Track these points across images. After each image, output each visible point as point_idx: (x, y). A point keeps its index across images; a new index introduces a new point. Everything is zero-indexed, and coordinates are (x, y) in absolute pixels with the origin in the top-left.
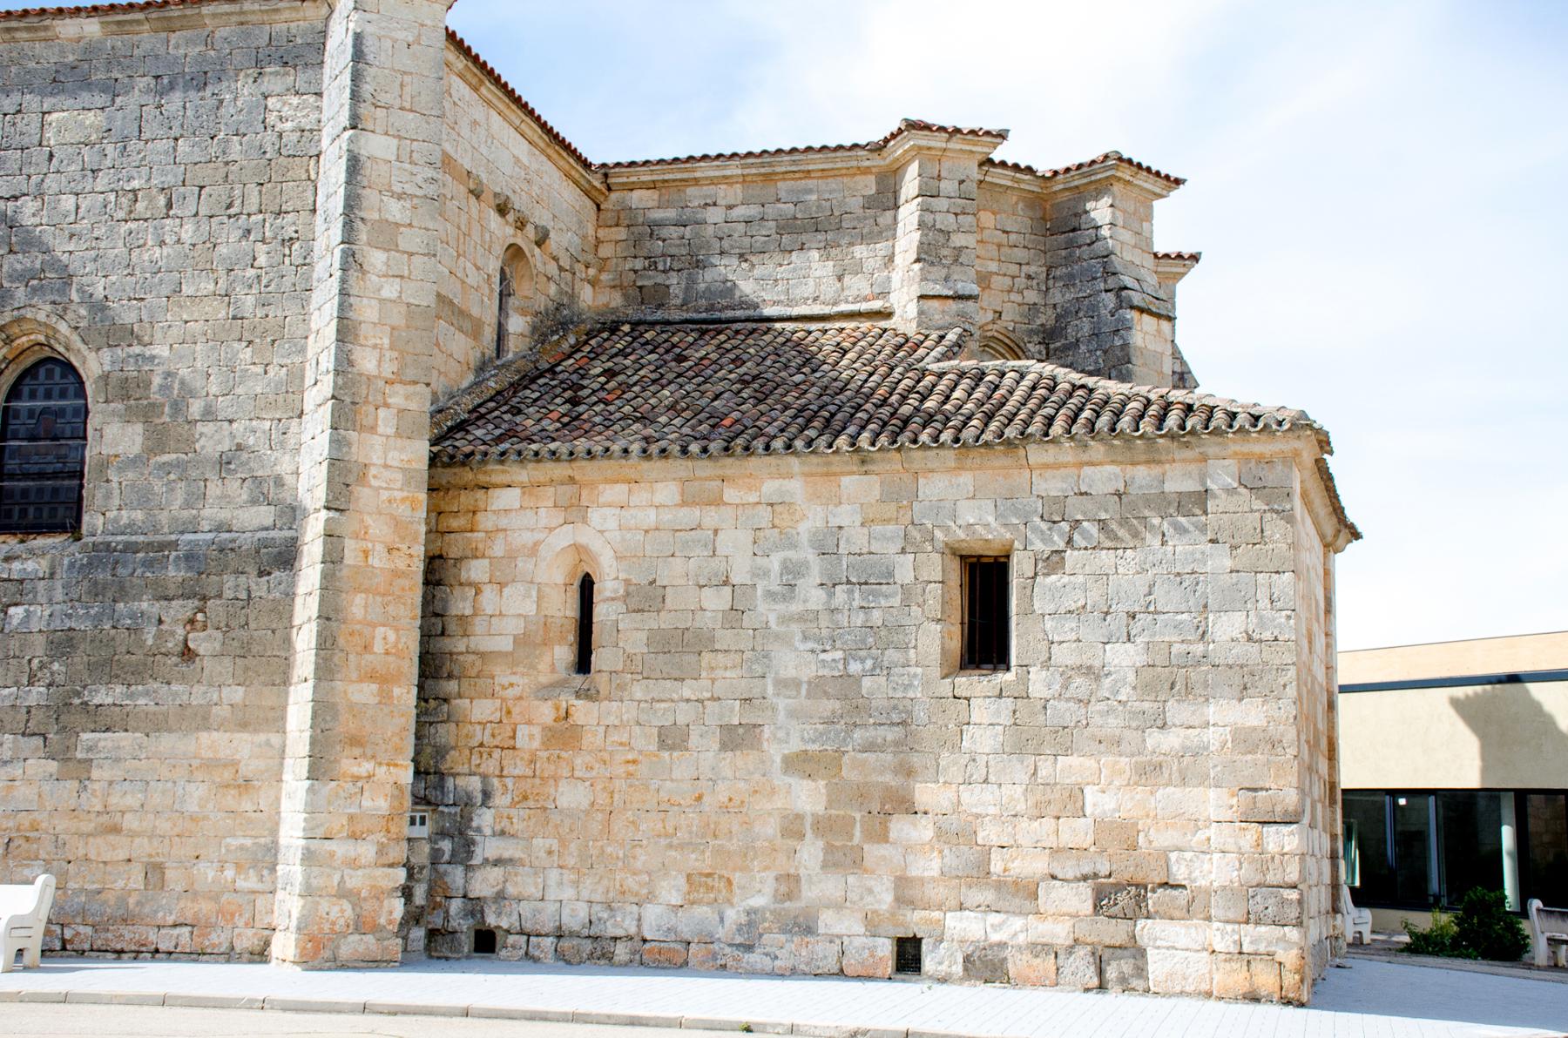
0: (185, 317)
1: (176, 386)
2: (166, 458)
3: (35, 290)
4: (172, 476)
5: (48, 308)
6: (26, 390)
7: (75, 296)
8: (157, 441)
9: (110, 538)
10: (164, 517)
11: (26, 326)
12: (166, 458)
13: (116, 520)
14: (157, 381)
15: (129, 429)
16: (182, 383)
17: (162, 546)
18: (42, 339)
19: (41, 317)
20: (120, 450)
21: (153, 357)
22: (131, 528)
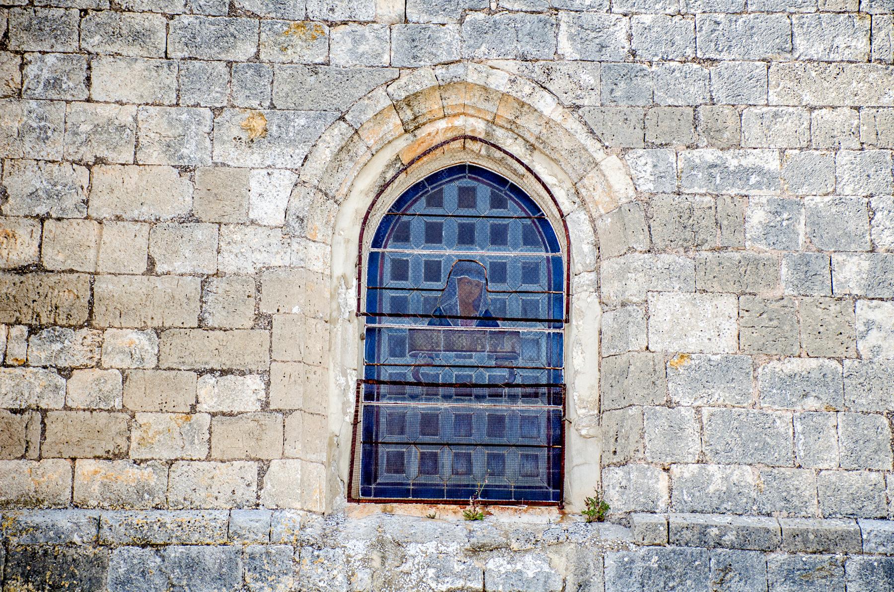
0: (808, 98)
1: (801, 228)
2: (793, 366)
3: (480, 31)
4: (811, 403)
5: (513, 66)
6: (417, 226)
7: (566, 47)
8: (770, 332)
9: (677, 520)
10: (805, 482)
11: (454, 99)
12: (793, 366)
13: (699, 484)
14: (757, 217)
15: (708, 305)
16: (815, 221)
17: (825, 544)
18: (479, 127)
19: (499, 82)
20: (692, 344)
21: (744, 173)
22: (729, 500)
